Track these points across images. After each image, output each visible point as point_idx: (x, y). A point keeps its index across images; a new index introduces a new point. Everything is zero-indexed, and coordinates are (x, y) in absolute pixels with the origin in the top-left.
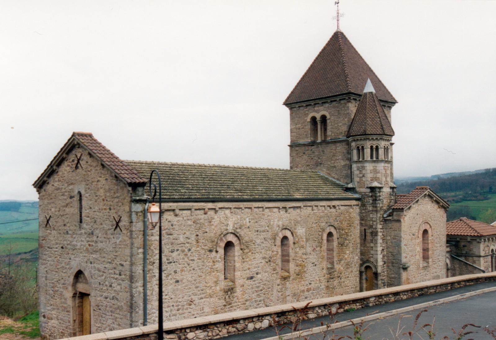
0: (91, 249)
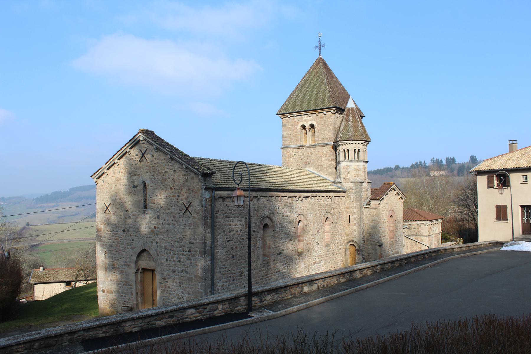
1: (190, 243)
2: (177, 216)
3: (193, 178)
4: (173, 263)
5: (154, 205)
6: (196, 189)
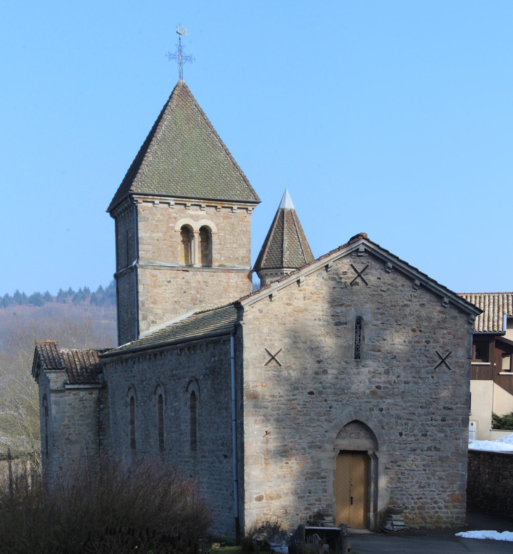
0: (382, 392)
1: (445, 408)
2: (423, 370)
3: (454, 318)
4: (413, 438)
5: (378, 353)
6: (459, 333)
